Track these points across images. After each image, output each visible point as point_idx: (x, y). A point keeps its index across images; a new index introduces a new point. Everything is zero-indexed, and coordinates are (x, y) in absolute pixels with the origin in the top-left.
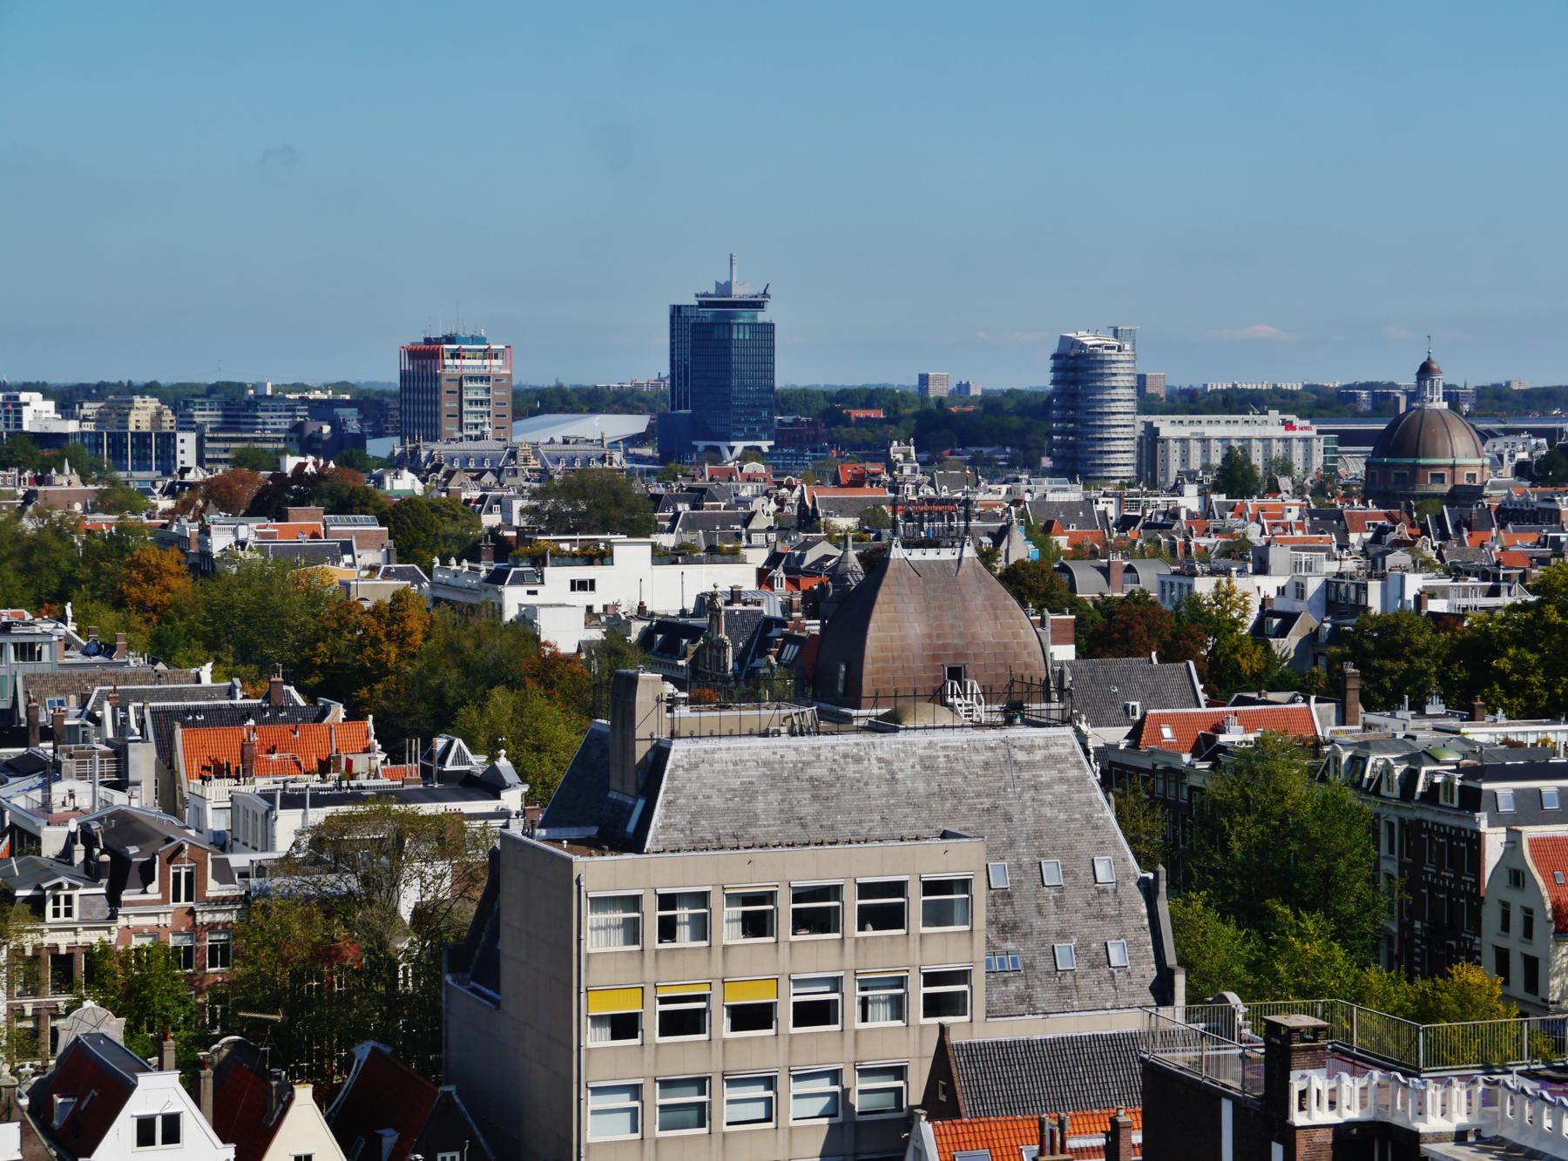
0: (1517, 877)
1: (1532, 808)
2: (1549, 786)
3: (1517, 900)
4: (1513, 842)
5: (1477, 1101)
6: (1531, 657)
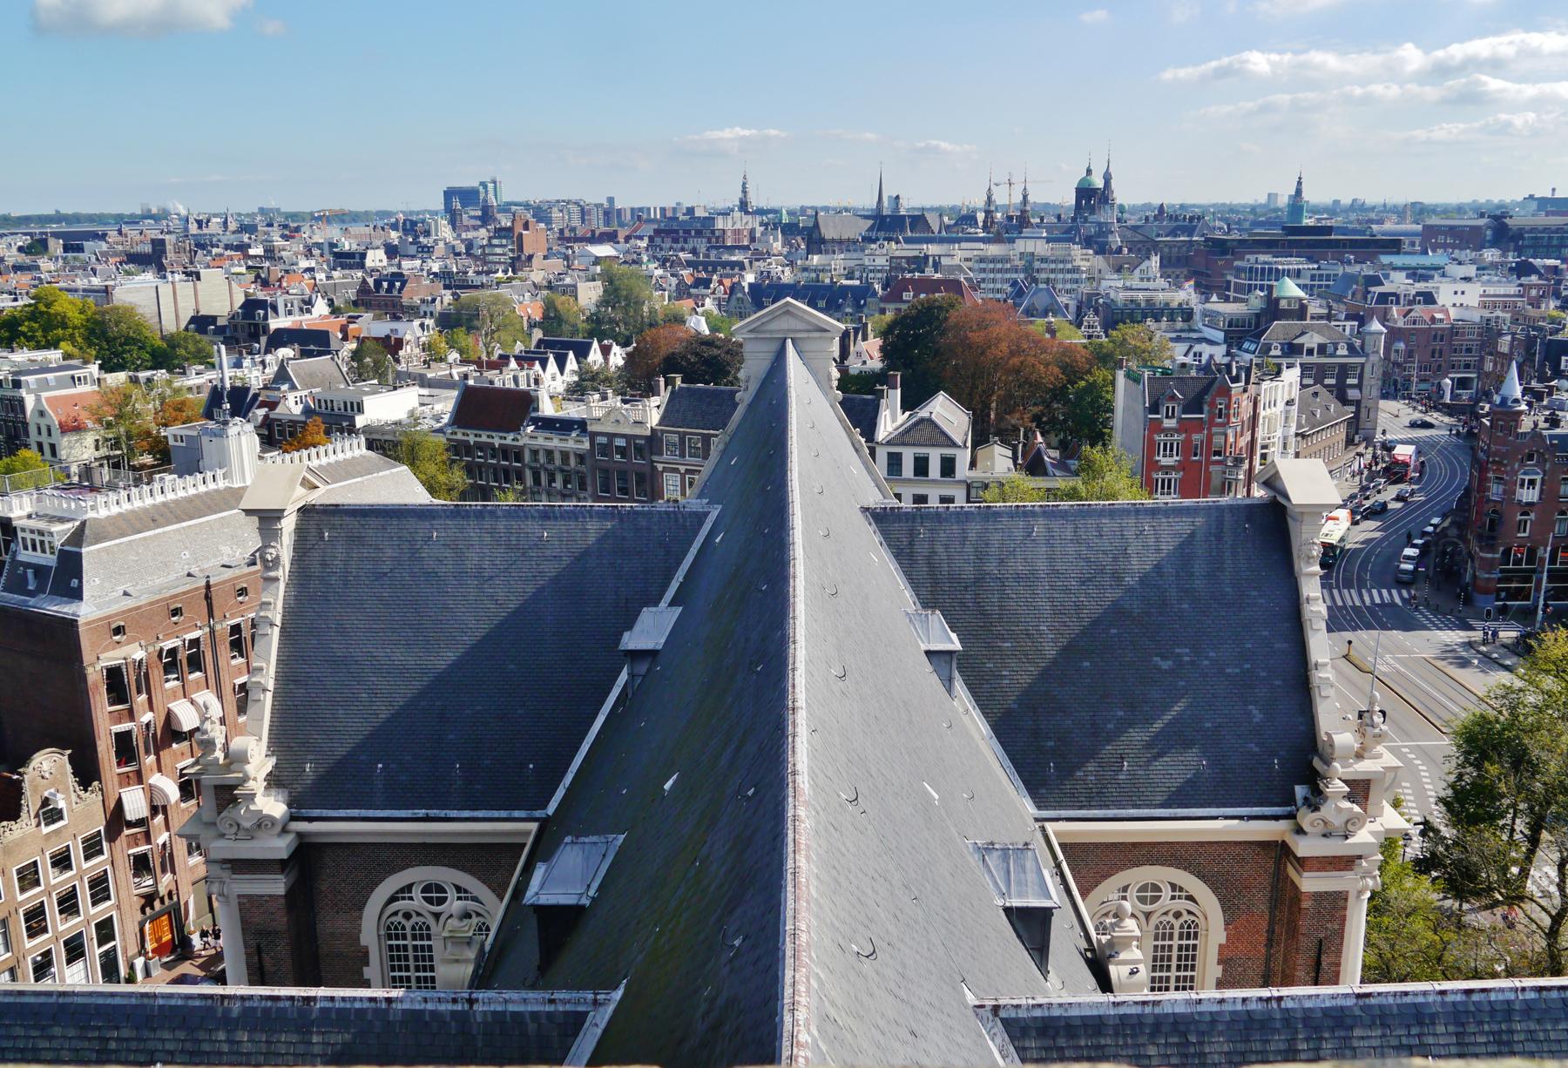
0: (42, 414)
1: (45, 385)
2: (50, 376)
3: (43, 422)
4: (38, 399)
5: (34, 502)
6: (36, 325)
